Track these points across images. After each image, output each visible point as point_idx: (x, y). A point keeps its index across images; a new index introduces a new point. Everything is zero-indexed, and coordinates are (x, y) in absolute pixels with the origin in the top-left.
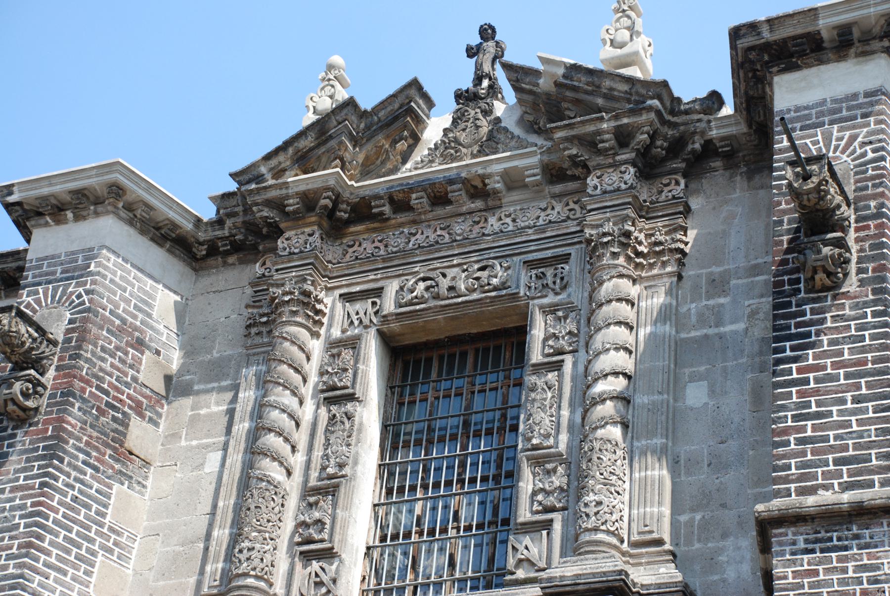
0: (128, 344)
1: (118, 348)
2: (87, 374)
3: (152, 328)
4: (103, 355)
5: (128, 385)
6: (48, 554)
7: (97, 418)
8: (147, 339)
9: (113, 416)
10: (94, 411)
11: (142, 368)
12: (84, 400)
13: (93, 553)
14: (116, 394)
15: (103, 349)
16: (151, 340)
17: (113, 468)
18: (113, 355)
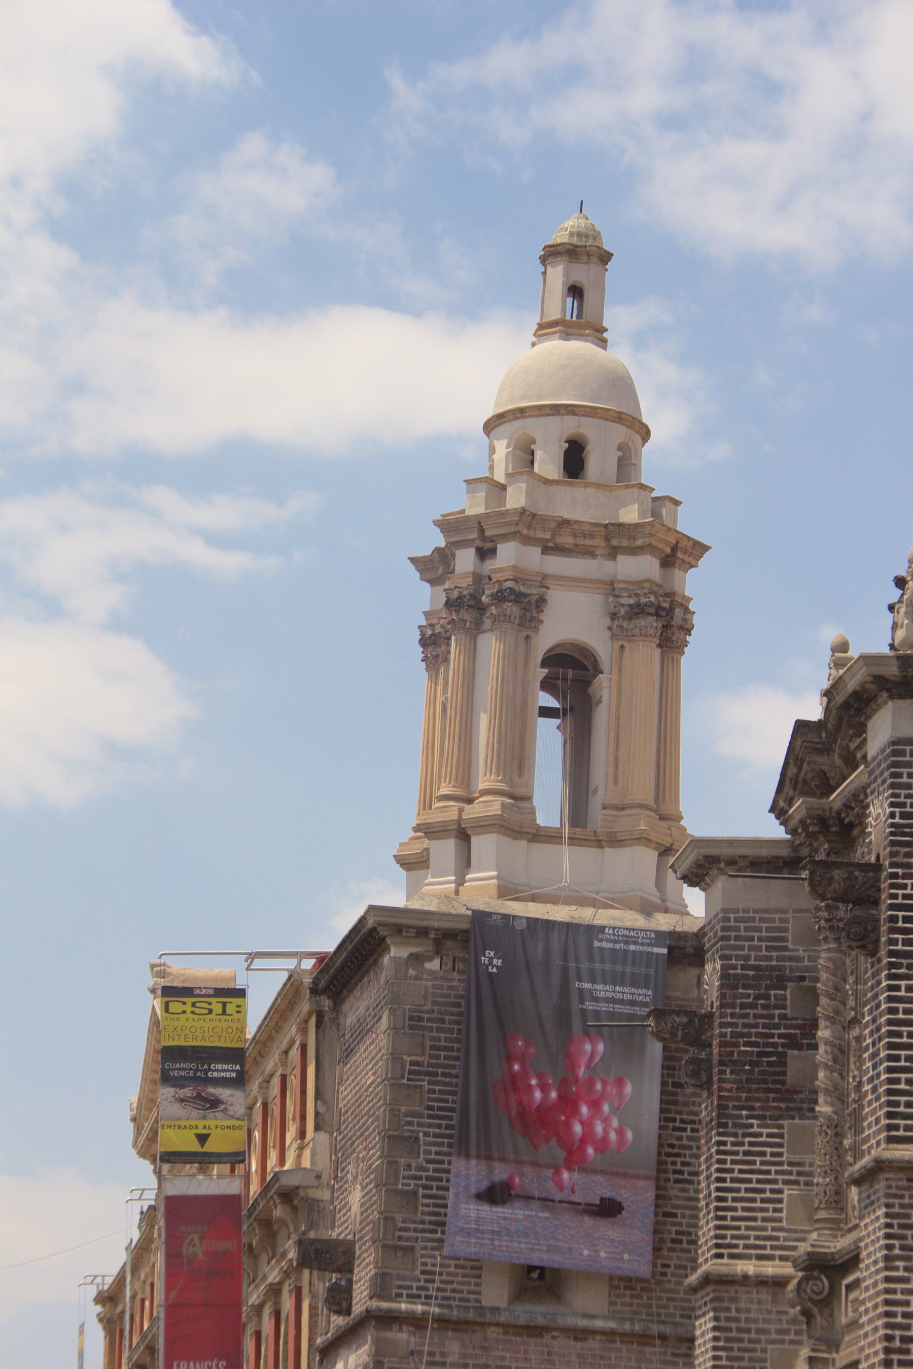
0: (769, 988)
1: (757, 997)
2: (731, 1037)
3: (791, 959)
4: (744, 1011)
5: (777, 1026)
6: (735, 1209)
7: (752, 1071)
8: (787, 972)
9: (768, 1062)
10: (747, 1067)
11: (788, 1002)
12: (734, 1063)
13: (780, 1191)
14: (765, 1040)
15: (743, 1006)
16: (792, 970)
17: (779, 1108)
18: (753, 1006)
